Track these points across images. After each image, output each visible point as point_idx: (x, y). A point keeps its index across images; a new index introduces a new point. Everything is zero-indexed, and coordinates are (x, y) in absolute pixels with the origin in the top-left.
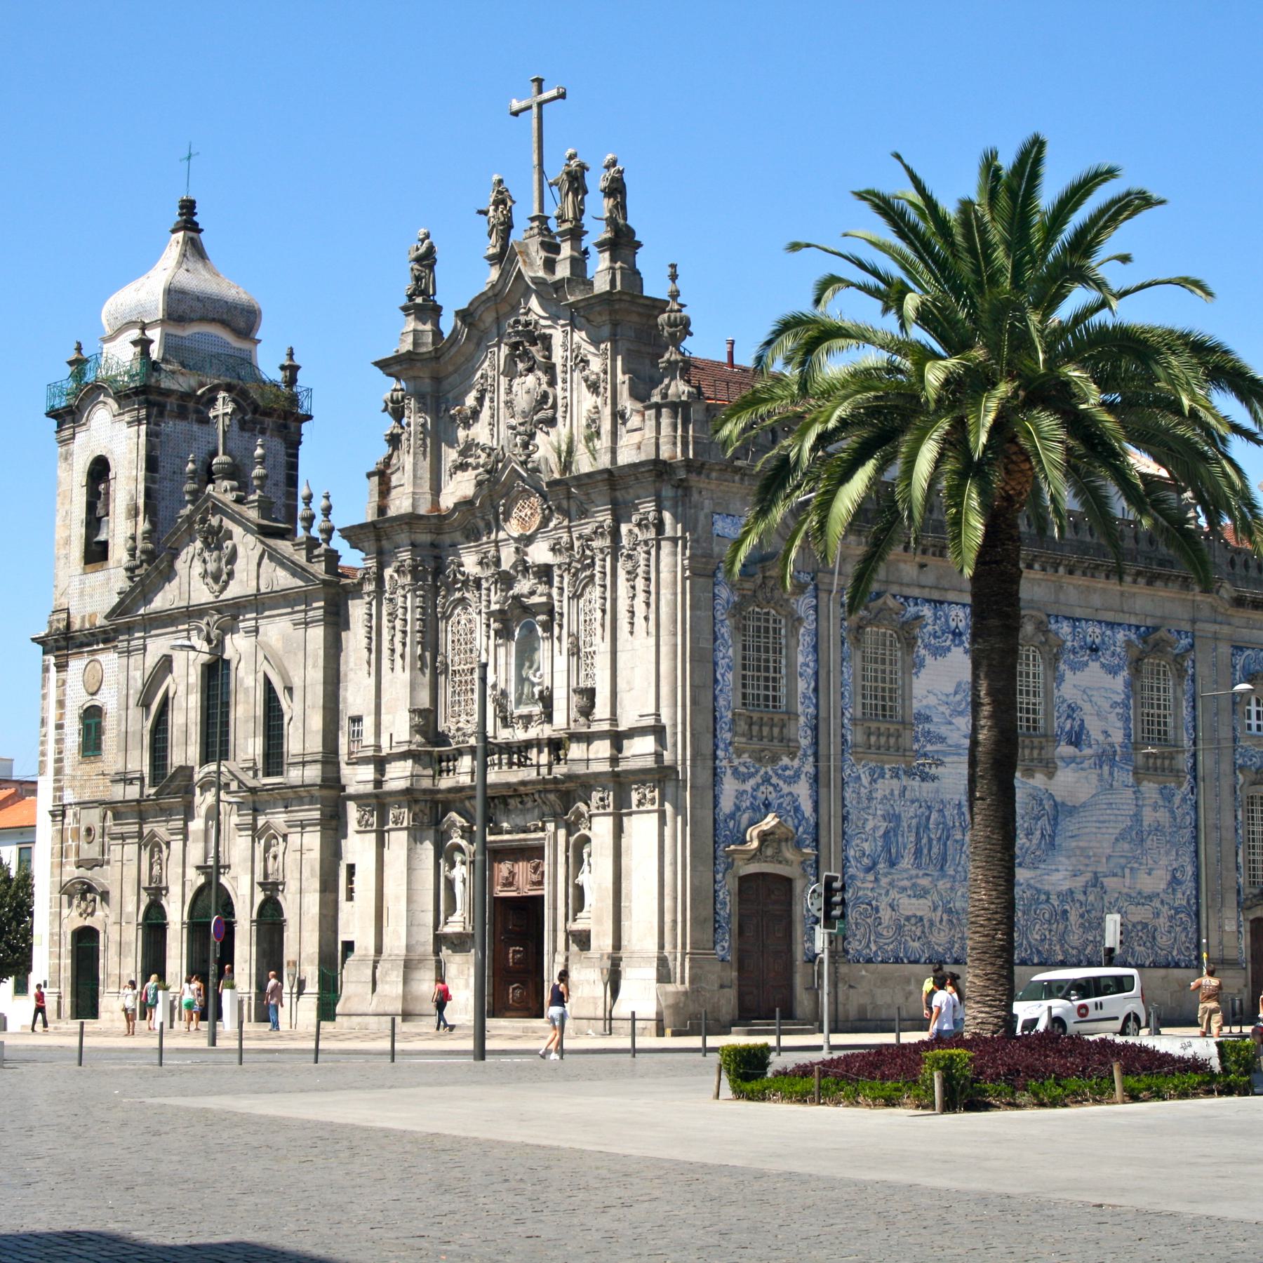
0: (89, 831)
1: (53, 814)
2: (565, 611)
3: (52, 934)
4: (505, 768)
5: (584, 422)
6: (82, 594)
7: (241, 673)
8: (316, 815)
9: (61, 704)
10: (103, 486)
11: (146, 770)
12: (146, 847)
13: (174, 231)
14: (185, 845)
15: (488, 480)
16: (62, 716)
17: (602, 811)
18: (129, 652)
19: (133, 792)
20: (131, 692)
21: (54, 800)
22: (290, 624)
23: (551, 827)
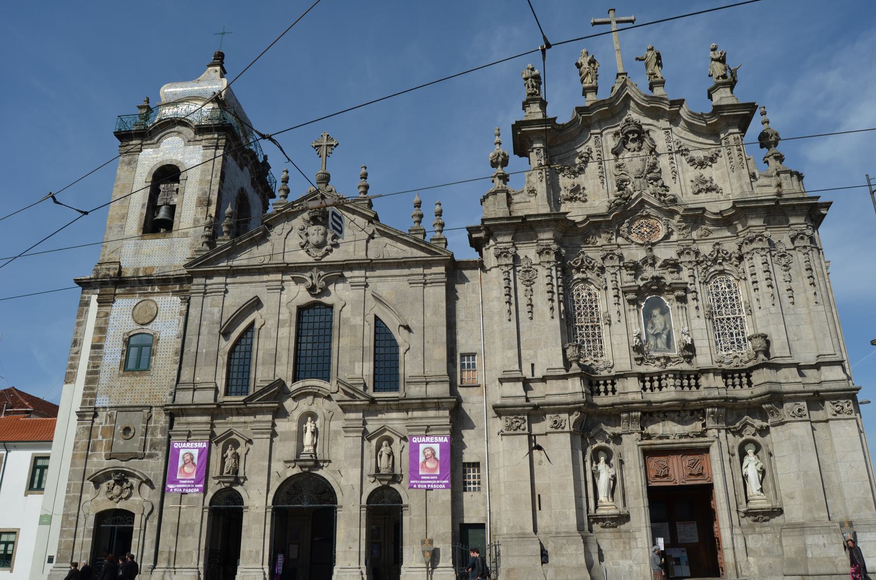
0: (127, 430)
1: (81, 415)
2: (698, 290)
3: (66, 516)
4: (679, 388)
5: (689, 184)
6: (137, 253)
7: (347, 313)
8: (447, 421)
9: (101, 330)
10: (162, 186)
11: (221, 384)
12: (217, 443)
13: (209, 66)
14: (272, 442)
15: (624, 203)
16: (101, 339)
17: (800, 419)
18: (205, 293)
19: (205, 397)
20: (204, 323)
21: (84, 402)
22: (406, 283)
23: (712, 433)
